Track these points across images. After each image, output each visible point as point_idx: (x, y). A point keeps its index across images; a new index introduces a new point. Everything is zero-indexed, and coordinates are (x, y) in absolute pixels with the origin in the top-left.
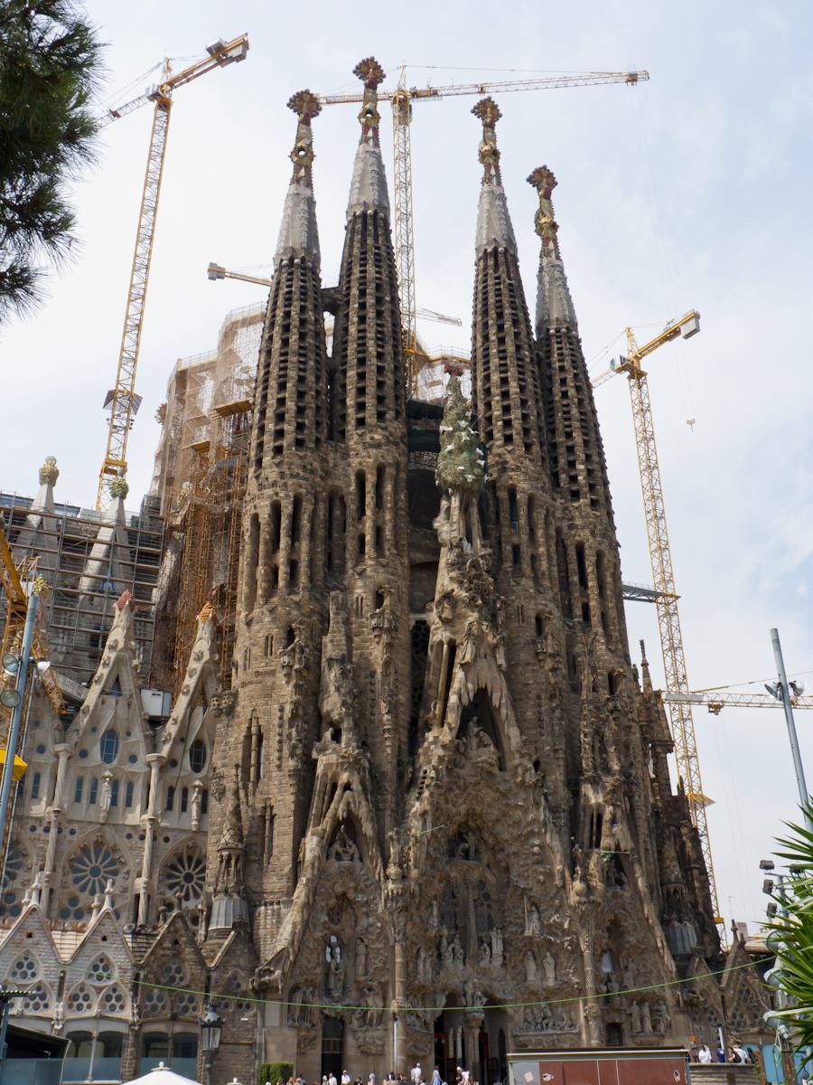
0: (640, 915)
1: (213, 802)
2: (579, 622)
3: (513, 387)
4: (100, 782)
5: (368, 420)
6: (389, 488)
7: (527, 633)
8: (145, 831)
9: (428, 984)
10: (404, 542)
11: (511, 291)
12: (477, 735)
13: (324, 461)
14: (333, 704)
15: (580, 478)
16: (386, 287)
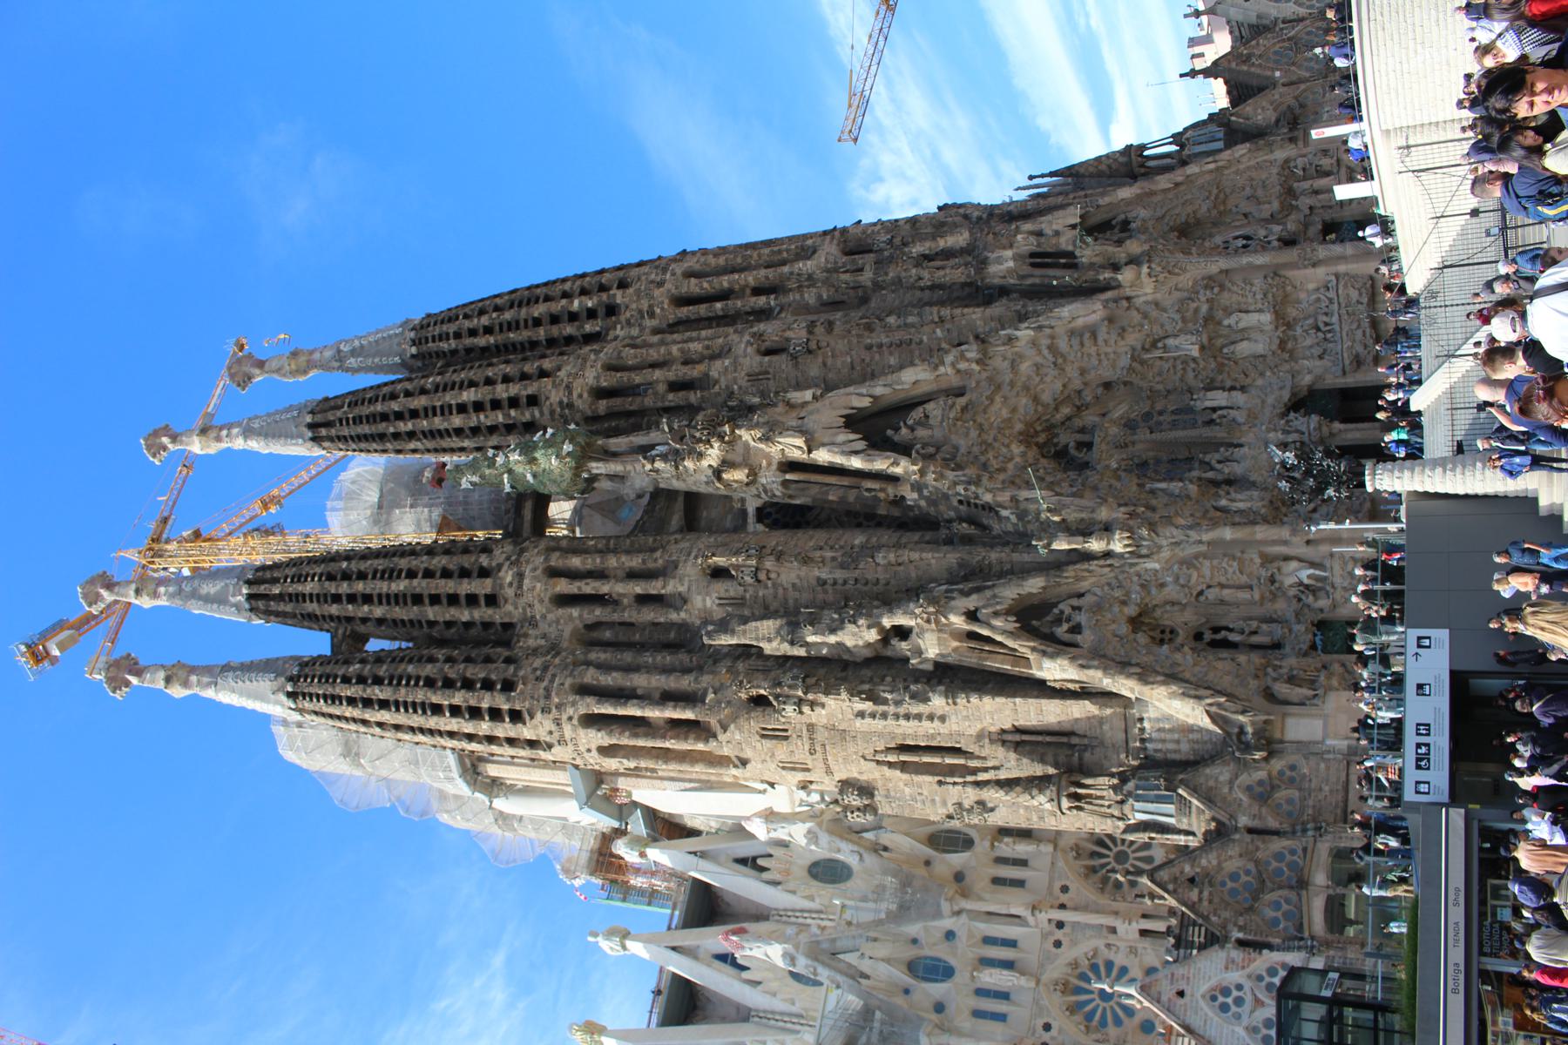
0: (1170, 195)
1: (998, 819)
2: (776, 299)
3: (468, 396)
4: (979, 985)
5: (488, 591)
6: (576, 562)
7: (784, 367)
8: (1050, 920)
9: (1268, 496)
10: (651, 540)
11: (356, 404)
12: (912, 429)
13: (535, 652)
14: (858, 636)
15: (590, 304)
16: (333, 567)
